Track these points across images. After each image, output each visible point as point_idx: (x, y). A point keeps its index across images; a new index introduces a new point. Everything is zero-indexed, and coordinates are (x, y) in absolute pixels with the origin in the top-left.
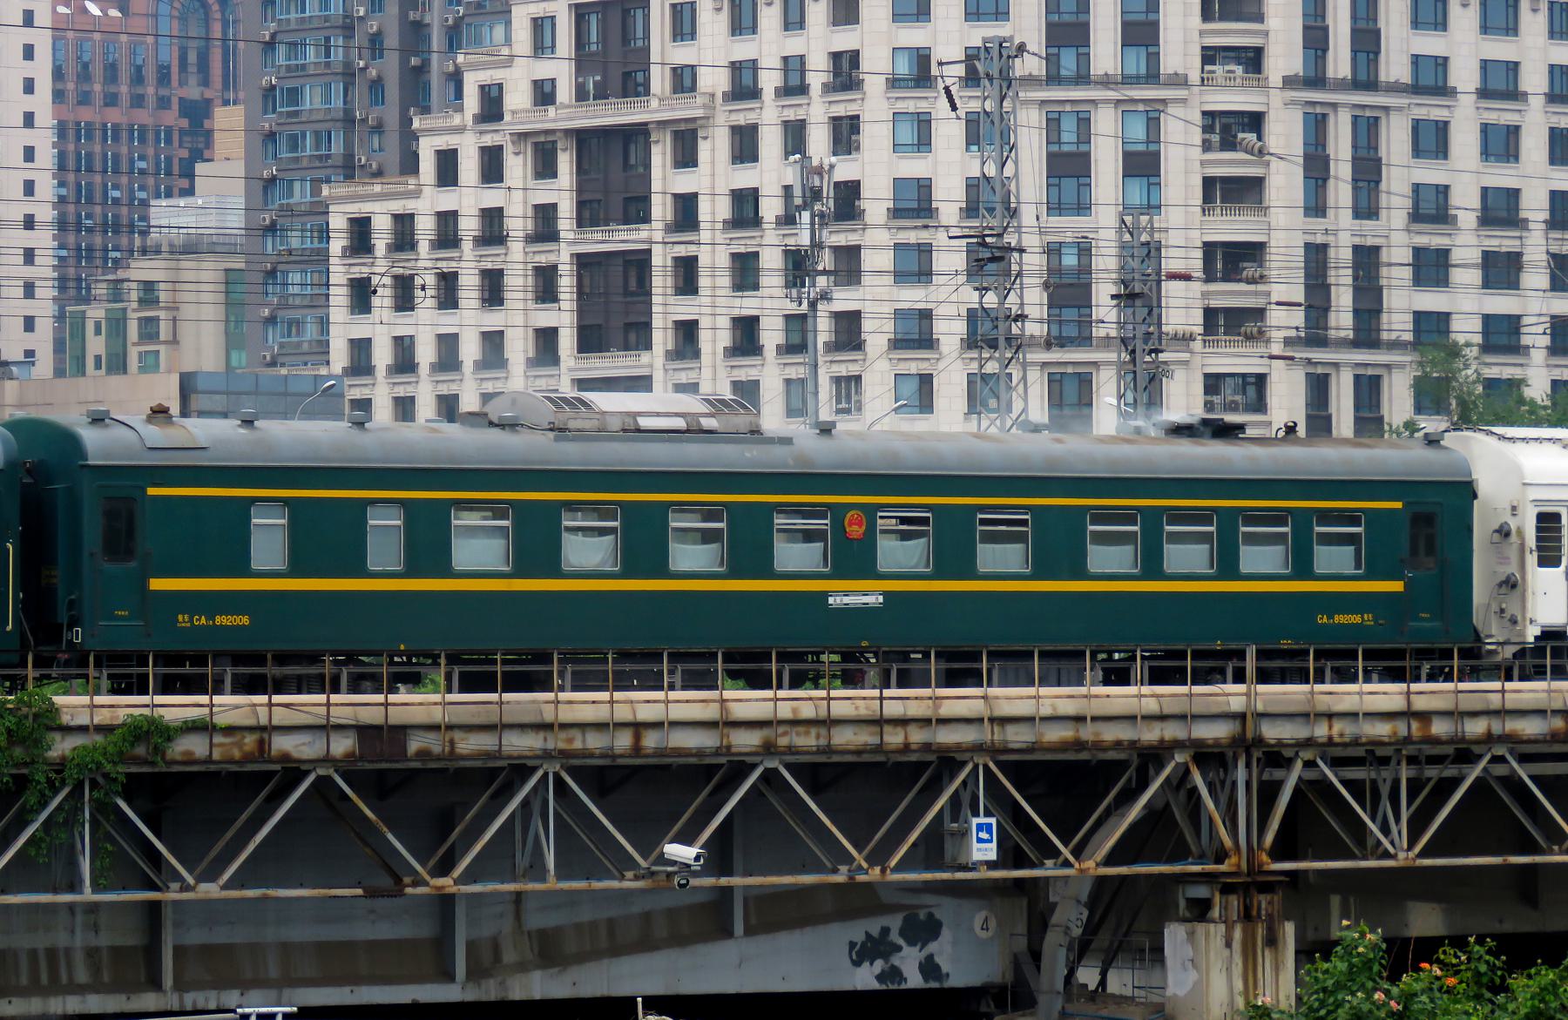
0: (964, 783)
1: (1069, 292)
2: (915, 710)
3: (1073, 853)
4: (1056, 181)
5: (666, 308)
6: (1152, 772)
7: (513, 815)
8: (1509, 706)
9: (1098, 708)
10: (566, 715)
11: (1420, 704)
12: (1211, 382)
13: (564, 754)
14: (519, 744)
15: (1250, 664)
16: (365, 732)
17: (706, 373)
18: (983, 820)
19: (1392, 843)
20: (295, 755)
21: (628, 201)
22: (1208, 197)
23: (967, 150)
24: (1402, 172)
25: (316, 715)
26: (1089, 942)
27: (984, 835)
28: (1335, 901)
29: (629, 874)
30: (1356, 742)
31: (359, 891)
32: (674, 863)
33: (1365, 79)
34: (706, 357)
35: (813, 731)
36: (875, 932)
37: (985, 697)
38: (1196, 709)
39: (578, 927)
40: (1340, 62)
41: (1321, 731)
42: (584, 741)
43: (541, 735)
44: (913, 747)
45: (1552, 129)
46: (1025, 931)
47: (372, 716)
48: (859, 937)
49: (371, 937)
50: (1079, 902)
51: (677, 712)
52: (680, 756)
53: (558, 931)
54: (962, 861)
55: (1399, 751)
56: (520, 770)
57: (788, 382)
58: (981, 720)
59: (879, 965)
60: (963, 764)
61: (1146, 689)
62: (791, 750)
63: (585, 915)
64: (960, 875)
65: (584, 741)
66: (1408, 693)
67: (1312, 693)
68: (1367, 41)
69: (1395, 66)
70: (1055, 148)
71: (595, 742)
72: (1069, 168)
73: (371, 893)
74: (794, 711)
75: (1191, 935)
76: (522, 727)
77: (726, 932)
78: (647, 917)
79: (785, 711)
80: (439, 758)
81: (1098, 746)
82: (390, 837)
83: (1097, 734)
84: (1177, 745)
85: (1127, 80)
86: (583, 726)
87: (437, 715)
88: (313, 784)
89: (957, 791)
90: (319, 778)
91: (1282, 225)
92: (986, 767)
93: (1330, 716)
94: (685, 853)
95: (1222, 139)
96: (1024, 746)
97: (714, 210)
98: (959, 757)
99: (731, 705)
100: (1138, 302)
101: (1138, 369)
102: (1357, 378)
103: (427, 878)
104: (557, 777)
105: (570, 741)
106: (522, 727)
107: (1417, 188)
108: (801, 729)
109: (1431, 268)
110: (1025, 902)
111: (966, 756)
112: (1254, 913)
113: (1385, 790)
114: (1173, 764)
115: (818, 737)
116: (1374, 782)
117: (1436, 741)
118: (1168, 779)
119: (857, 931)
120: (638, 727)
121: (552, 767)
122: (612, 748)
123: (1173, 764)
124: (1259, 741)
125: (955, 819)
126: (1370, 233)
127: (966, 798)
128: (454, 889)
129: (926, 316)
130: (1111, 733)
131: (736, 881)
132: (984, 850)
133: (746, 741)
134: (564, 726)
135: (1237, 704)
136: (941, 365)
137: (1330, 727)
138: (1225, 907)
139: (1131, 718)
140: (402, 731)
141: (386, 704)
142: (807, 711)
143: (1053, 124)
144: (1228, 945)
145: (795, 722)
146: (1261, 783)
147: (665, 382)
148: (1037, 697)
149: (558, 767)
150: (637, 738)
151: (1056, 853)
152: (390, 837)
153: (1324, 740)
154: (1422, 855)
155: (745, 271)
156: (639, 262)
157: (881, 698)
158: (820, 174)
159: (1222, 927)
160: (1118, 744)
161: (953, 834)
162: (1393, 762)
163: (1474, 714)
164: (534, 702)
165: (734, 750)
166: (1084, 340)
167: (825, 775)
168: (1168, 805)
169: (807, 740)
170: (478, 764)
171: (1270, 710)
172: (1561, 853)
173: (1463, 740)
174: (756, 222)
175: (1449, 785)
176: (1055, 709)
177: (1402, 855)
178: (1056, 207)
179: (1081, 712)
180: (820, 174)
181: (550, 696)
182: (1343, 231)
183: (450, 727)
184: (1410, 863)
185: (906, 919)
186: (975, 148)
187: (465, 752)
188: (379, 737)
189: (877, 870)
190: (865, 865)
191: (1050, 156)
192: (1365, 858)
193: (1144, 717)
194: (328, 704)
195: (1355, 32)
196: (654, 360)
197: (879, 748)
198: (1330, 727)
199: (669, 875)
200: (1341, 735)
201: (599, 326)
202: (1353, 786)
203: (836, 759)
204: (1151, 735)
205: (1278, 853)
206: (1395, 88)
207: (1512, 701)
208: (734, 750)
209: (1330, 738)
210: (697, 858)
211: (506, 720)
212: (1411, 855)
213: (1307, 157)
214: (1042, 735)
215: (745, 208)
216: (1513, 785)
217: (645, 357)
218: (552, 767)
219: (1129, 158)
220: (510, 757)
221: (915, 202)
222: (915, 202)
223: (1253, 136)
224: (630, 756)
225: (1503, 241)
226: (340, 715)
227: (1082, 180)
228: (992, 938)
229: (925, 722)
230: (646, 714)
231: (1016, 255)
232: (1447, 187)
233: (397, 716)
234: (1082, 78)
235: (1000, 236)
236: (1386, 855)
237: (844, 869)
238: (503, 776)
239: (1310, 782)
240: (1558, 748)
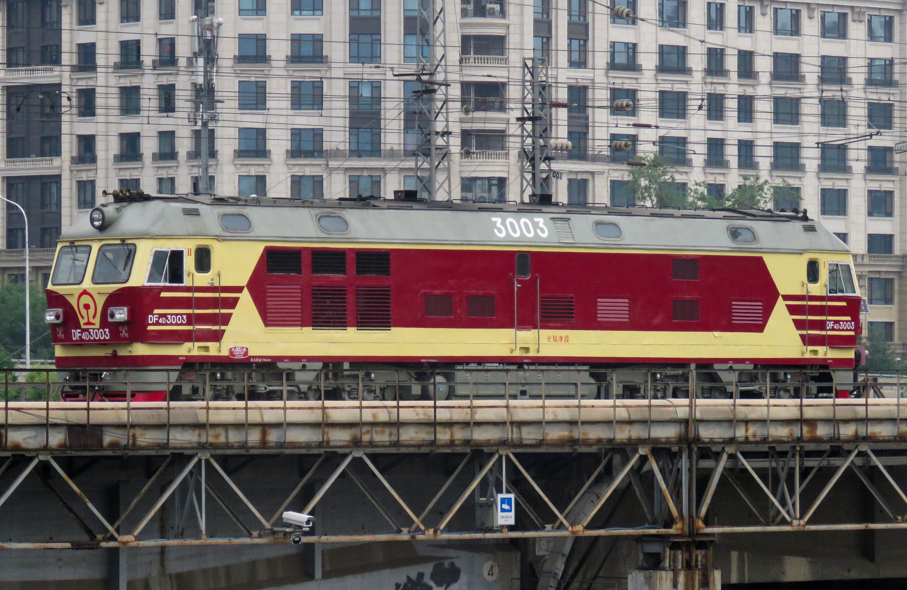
0: (491, 470)
1: (365, 117)
2: (458, 415)
3: (565, 518)
4: (356, 37)
5: (71, 126)
6: (617, 459)
7: (174, 491)
8: (870, 416)
9: (586, 415)
10: (215, 417)
11: (809, 413)
12: (467, 182)
13: (214, 446)
14: (180, 438)
15: (693, 383)
16: (72, 428)
17: (101, 173)
18: (505, 495)
19: (788, 512)
20: (24, 445)
21: (44, 48)
22: (465, 50)
23: (292, 14)
24: (605, 33)
25: (38, 416)
26: (568, 584)
27: (506, 507)
28: (734, 555)
29: (255, 533)
30: (765, 440)
31: (68, 545)
32: (289, 525)
34: (100, 162)
35: (387, 430)
36: (414, 576)
37: (507, 407)
38: (655, 416)
39: (205, 571)
41: (740, 433)
42: (227, 437)
43: (197, 432)
44: (457, 442)
45: (709, 4)
46: (519, 576)
47: (78, 417)
48: (403, 580)
49: (58, 578)
50: (564, 555)
51: (292, 416)
52: (294, 448)
53: (190, 574)
54: (488, 525)
55: (795, 447)
56: (180, 458)
57: (160, 180)
58: (504, 423)
60: (491, 455)
61: (619, 402)
62: (371, 444)
63: (210, 563)
64: (489, 535)
65: (227, 437)
66: (801, 405)
67: (734, 405)
70: (355, 13)
71: (234, 437)
72: (365, 30)
73: (77, 546)
74: (374, 416)
75: (649, 581)
76: (183, 426)
77: (310, 576)
78: (253, 564)
79: (367, 416)
80: (125, 447)
81: (586, 442)
82: (90, 505)
83: (585, 434)
84: (642, 442)
86: (226, 426)
87: (124, 417)
88: (35, 468)
89: (486, 476)
90: (40, 462)
92: (508, 457)
93: (747, 422)
94: (301, 518)
95: (475, 7)
96: (534, 442)
97: (107, 54)
98: (486, 450)
99: (329, 411)
100: (538, 122)
101: (537, 172)
102: (570, 180)
103: (116, 535)
104: (207, 461)
105: (217, 436)
106: (183, 426)
107: (613, 45)
108: (379, 429)
109: (624, 102)
110: (519, 555)
111: (495, 448)
112: (693, 564)
113: (783, 475)
114: (637, 456)
115: (390, 435)
116: (774, 469)
117: (819, 440)
118: (632, 467)
119: (401, 575)
120: (265, 427)
121: (204, 455)
122: (246, 442)
123: (637, 456)
124: (697, 439)
125: (483, 495)
126: (580, 75)
127: (491, 479)
128: (135, 544)
129: (261, 133)
130: (594, 433)
131: (324, 538)
132: (505, 517)
133: (340, 437)
134: (214, 426)
135: (682, 413)
136: (272, 169)
137: (747, 430)
138: (674, 560)
139: (608, 423)
140: (99, 428)
141: (88, 409)
142: (383, 416)
144: (675, 585)
145: (374, 424)
146: (697, 469)
147: (71, 179)
148: (543, 407)
149: (208, 455)
150: (264, 434)
151: (553, 519)
152: (90, 505)
153: (742, 439)
154: (810, 522)
155: (130, 100)
156: (52, 91)
157: (435, 407)
158: (211, 30)
159: (671, 574)
160: (599, 441)
161: (482, 505)
162: (789, 455)
163: (846, 421)
164: (192, 408)
165: (331, 444)
166: (375, 151)
167: (393, 461)
168: (630, 483)
169: (382, 437)
170: (153, 453)
171: (705, 417)
172: (903, 521)
173: (839, 439)
174: (138, 64)
175: (825, 474)
176: (555, 416)
177: (795, 522)
178: (355, 57)
179: (577, 418)
180: (211, 30)
181: (203, 404)
182: (562, 75)
183: (133, 426)
184: (801, 528)
185: (435, 567)
186: (297, 13)
187: (143, 444)
188: (83, 433)
189: (431, 531)
190: (422, 527)
191: (352, 19)
192: (768, 524)
193: (618, 422)
194: (47, 409)
196: (62, 165)
197: (433, 443)
198: (747, 430)
199: (285, 534)
200: (754, 436)
201: (23, 138)
202: (762, 473)
203: (403, 450)
204: (622, 434)
205: (707, 522)
207: (873, 412)
208: (331, 444)
209: (747, 438)
210: (308, 522)
211: (173, 421)
212: (802, 522)
213: (536, 22)
214: (547, 434)
215: (130, 54)
216: (872, 472)
217: (56, 162)
218: (204, 455)
219: (407, 19)
220: (175, 448)
221: (254, 51)
222: (254, 51)
223: (497, 7)
224: (259, 448)
225: (673, 83)
226: (56, 417)
227: (374, 37)
228: (495, 581)
229: (466, 424)
230: (270, 417)
231: (443, 88)
232: (635, 45)
233: (96, 418)
235: (431, 74)
236: (784, 522)
237: (405, 530)
238: (160, 464)
239: (729, 469)
240: (903, 446)
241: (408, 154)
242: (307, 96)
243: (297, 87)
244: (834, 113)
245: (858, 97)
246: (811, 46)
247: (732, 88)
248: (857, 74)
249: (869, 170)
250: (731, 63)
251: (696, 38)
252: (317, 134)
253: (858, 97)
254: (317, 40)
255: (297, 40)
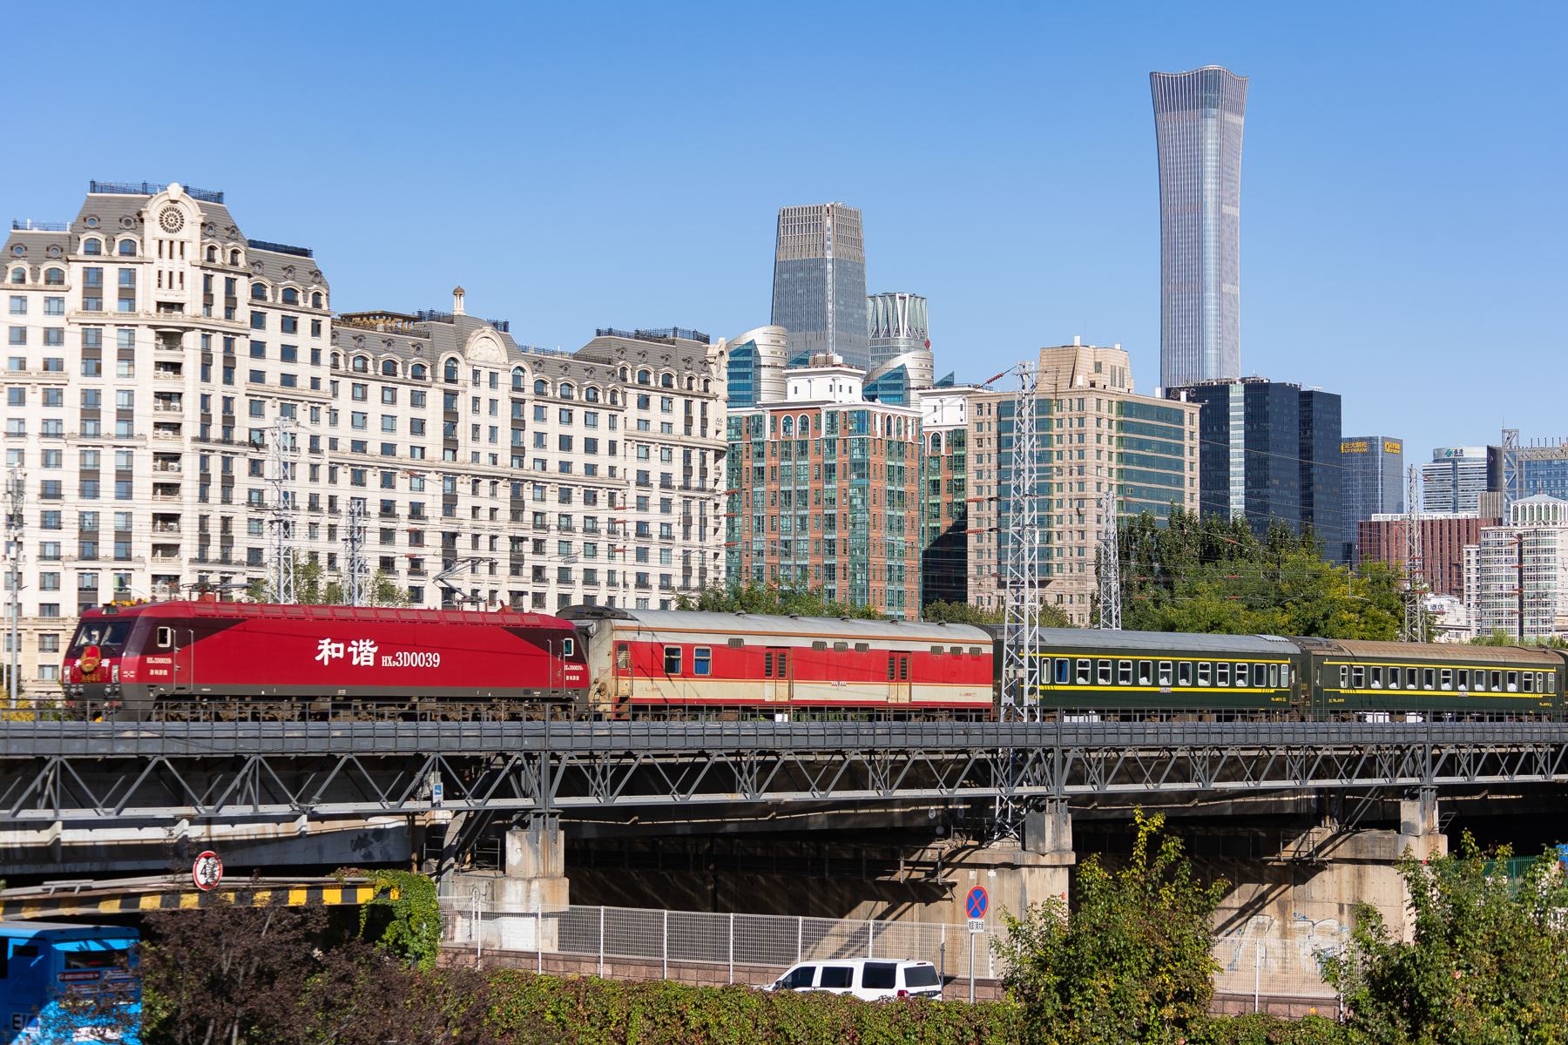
33: (227, 439)
40: (216, 431)
59: (363, 851)
68: (229, 422)
69: (240, 434)
85: (118, 436)
91: (187, 505)
113: (599, 770)
143: (83, 454)
166: (94, 558)
178: (83, 493)
191: (82, 472)
195: (224, 418)
206: (242, 444)
218: (260, 757)
234: (97, 435)
241: (117, 559)
242: (51, 521)
243: (45, 514)
244: (387, 536)
245: (403, 524)
246: (373, 493)
247: (325, 520)
248: (403, 510)
249: (410, 573)
250: (324, 503)
251: (302, 487)
252: (57, 545)
253: (403, 524)
254: (58, 484)
255: (45, 484)
